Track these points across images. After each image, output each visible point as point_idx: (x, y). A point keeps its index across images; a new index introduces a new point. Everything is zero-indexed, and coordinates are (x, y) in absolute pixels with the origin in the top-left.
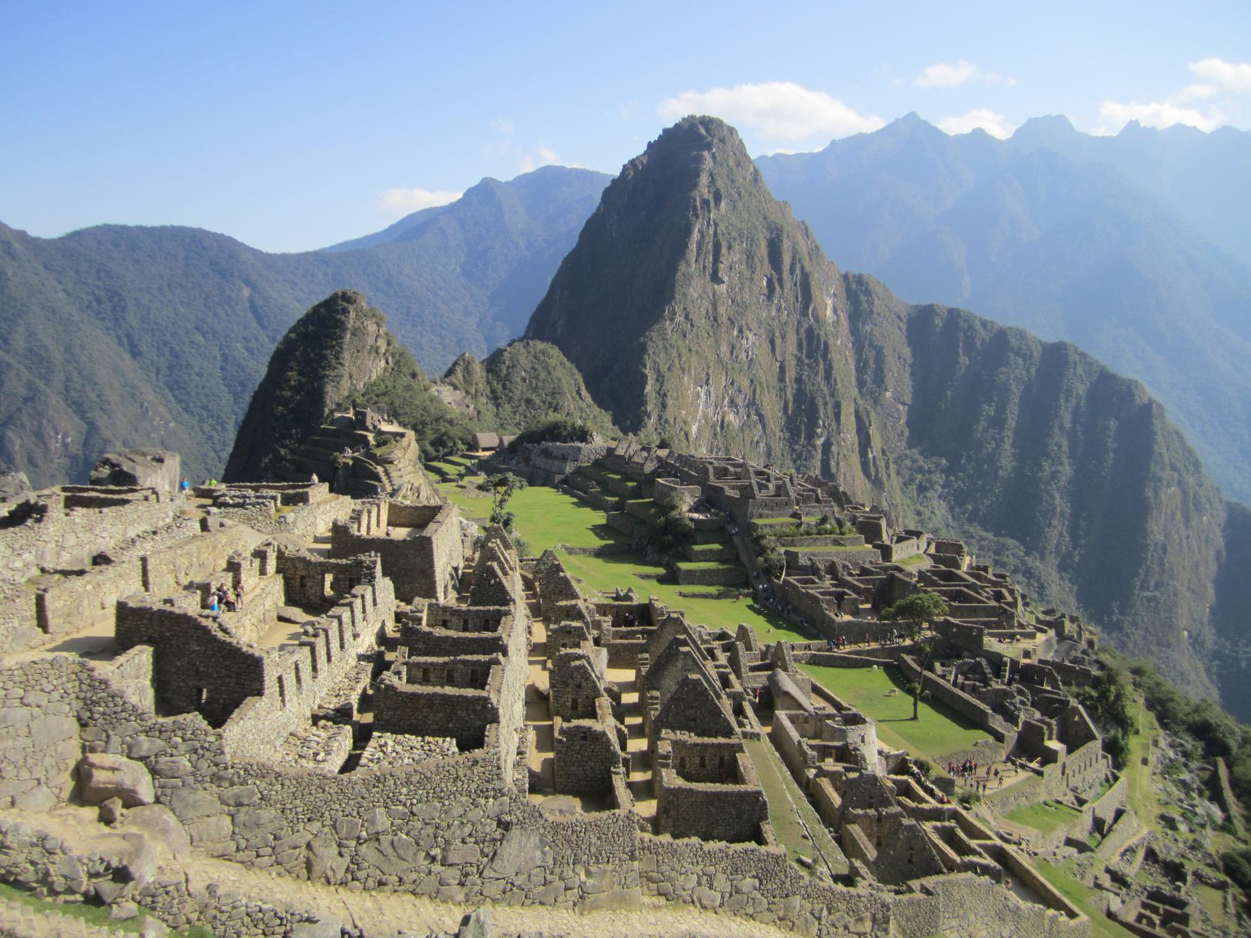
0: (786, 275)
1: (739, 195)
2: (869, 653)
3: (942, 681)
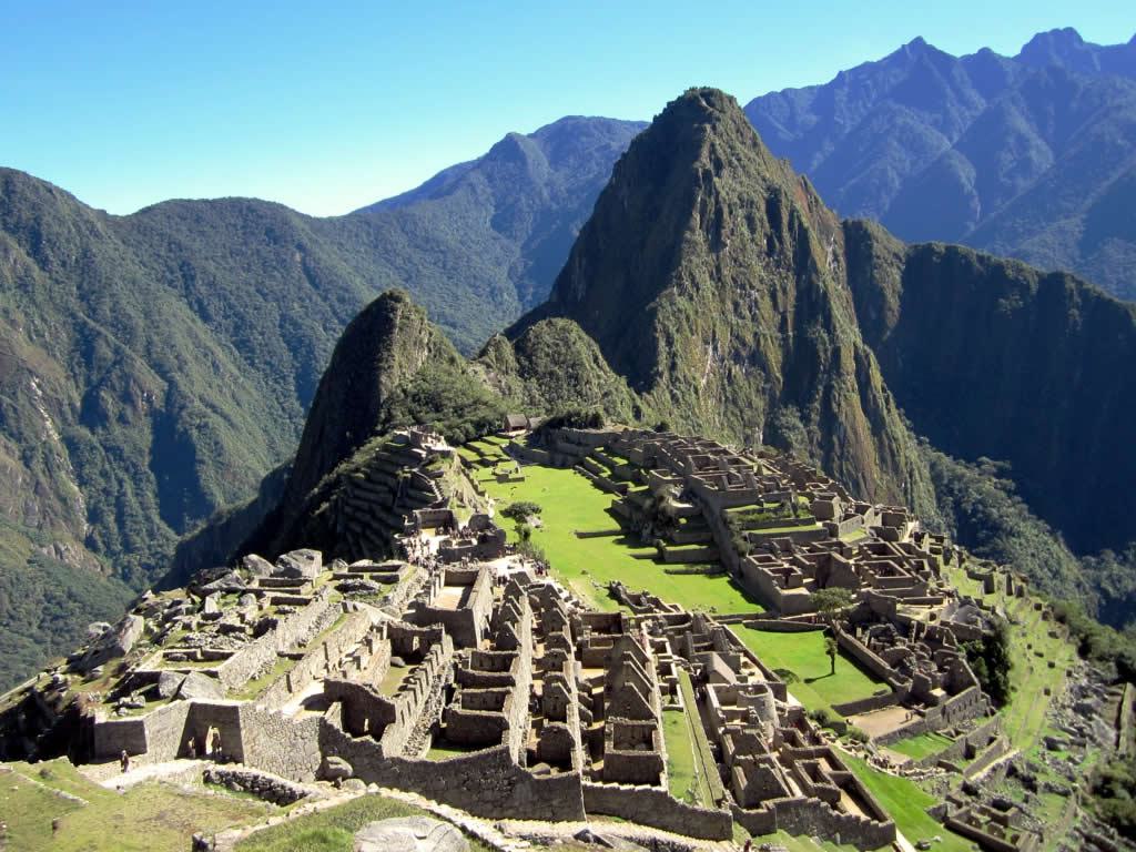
0: (786, 234)
1: (739, 160)
2: (809, 619)
3: (858, 643)
